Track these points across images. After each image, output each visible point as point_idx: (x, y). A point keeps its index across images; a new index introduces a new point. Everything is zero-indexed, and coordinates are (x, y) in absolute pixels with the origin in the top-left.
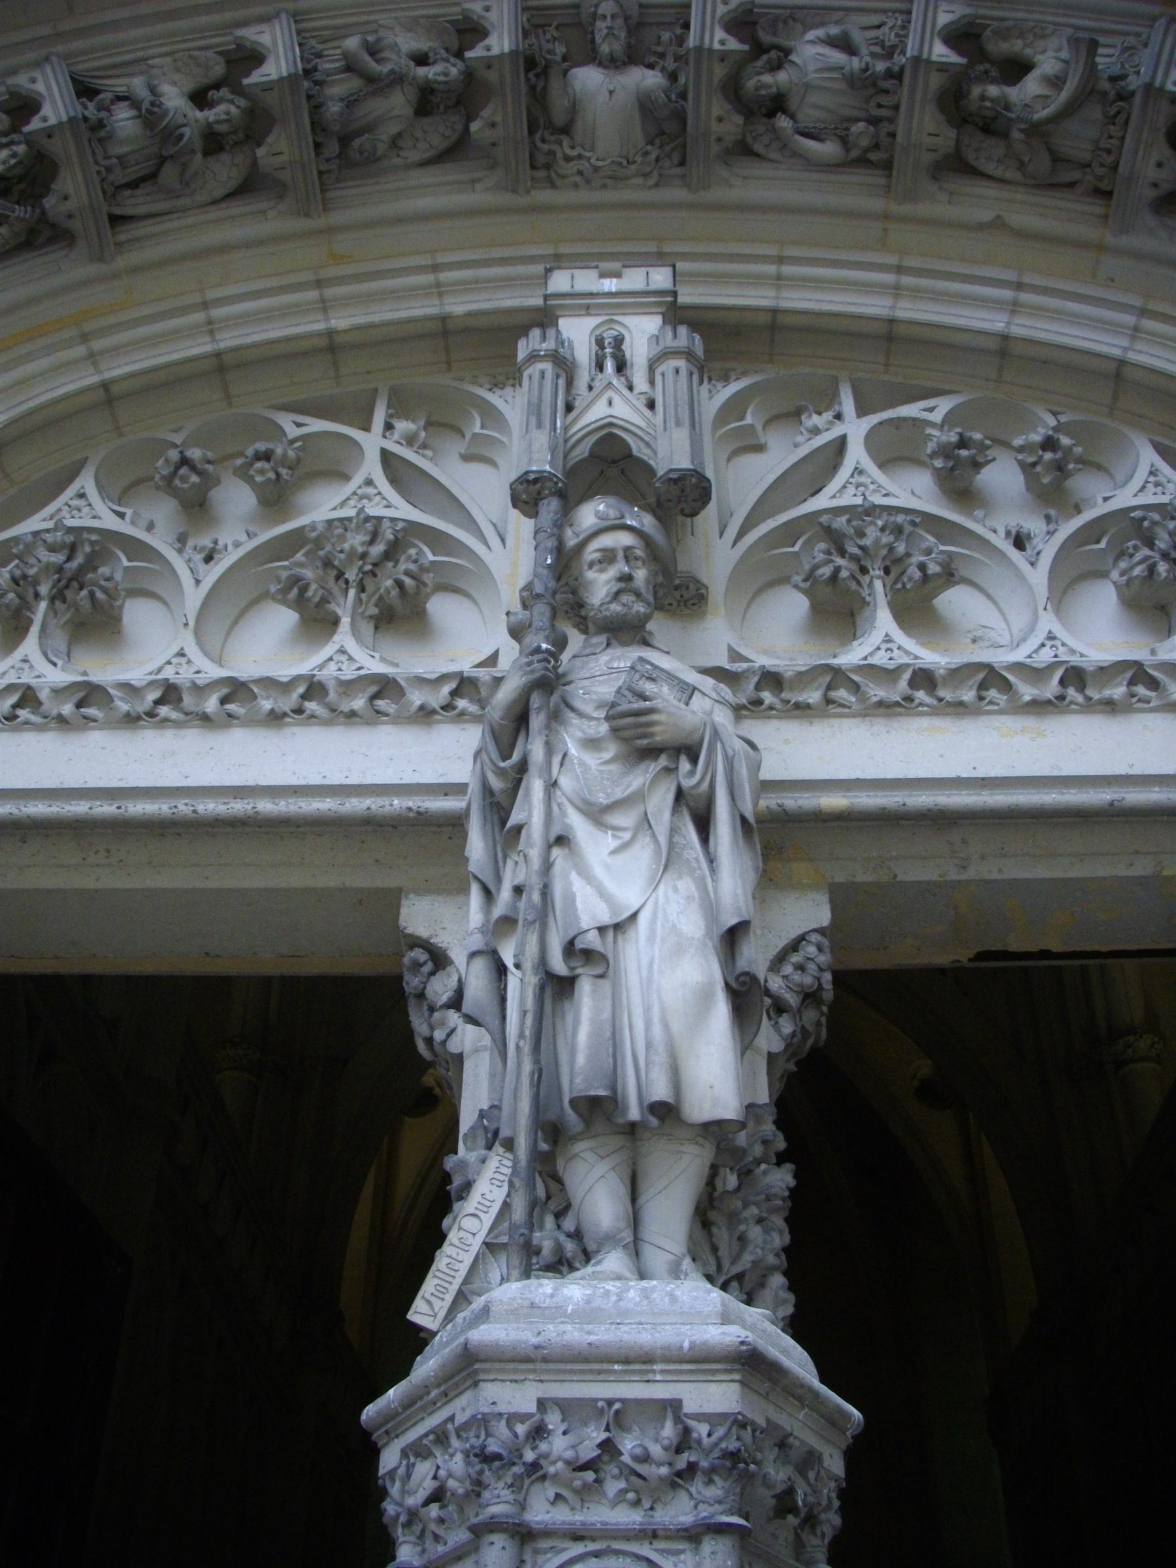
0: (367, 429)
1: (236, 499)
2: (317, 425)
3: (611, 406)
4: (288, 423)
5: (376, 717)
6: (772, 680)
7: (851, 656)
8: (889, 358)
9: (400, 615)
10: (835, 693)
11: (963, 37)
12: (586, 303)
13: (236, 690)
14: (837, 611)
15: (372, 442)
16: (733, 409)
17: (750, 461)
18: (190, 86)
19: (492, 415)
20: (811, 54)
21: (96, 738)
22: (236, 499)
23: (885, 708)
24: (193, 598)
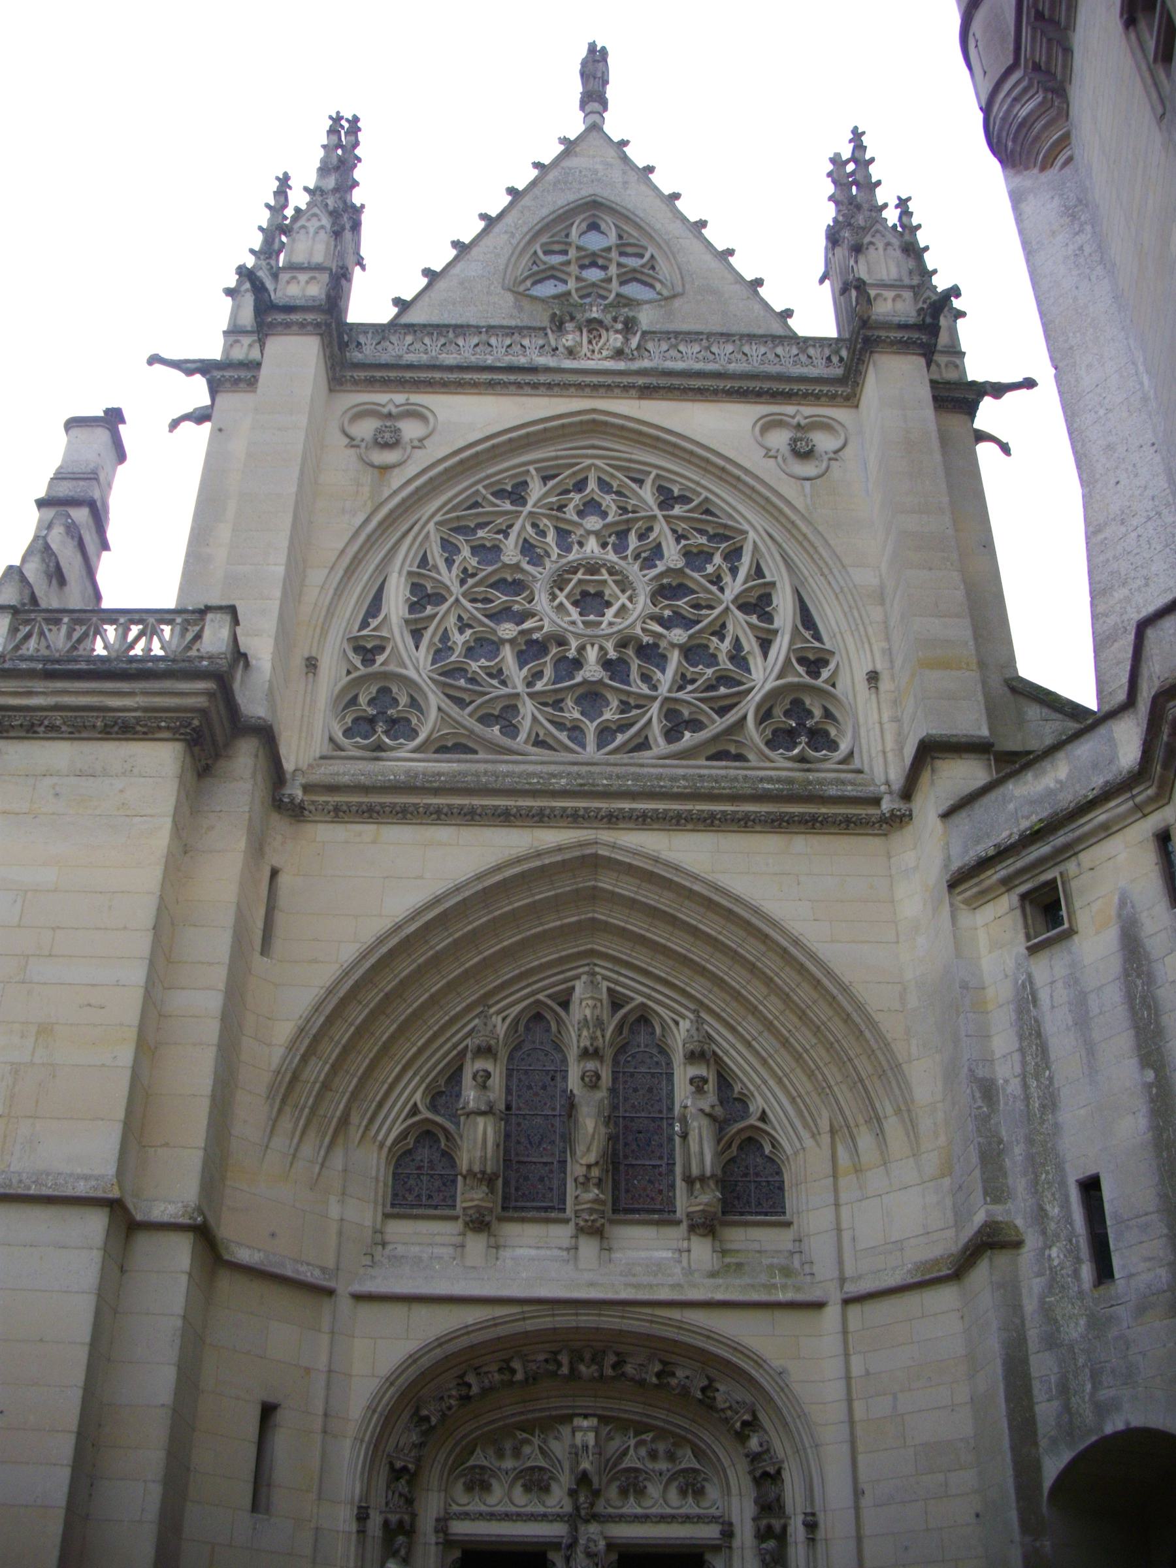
0: (533, 1435)
1: (508, 1452)
2: (525, 1435)
3: (585, 1465)
4: (518, 1433)
5: (542, 1521)
6: (610, 1516)
7: (624, 1510)
8: (640, 1428)
9: (546, 1489)
10: (620, 1518)
11: (659, 1375)
12: (580, 1429)
13: (518, 1515)
14: (624, 1492)
15: (536, 1441)
16: (609, 1433)
17: (612, 1442)
18: (496, 1368)
19: (559, 1431)
20: (629, 1369)
21: (494, 1523)
22: (508, 1452)
23: (630, 1522)
24: (506, 1486)
